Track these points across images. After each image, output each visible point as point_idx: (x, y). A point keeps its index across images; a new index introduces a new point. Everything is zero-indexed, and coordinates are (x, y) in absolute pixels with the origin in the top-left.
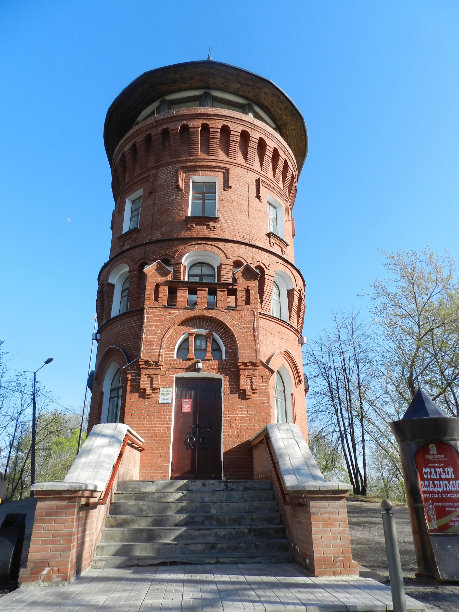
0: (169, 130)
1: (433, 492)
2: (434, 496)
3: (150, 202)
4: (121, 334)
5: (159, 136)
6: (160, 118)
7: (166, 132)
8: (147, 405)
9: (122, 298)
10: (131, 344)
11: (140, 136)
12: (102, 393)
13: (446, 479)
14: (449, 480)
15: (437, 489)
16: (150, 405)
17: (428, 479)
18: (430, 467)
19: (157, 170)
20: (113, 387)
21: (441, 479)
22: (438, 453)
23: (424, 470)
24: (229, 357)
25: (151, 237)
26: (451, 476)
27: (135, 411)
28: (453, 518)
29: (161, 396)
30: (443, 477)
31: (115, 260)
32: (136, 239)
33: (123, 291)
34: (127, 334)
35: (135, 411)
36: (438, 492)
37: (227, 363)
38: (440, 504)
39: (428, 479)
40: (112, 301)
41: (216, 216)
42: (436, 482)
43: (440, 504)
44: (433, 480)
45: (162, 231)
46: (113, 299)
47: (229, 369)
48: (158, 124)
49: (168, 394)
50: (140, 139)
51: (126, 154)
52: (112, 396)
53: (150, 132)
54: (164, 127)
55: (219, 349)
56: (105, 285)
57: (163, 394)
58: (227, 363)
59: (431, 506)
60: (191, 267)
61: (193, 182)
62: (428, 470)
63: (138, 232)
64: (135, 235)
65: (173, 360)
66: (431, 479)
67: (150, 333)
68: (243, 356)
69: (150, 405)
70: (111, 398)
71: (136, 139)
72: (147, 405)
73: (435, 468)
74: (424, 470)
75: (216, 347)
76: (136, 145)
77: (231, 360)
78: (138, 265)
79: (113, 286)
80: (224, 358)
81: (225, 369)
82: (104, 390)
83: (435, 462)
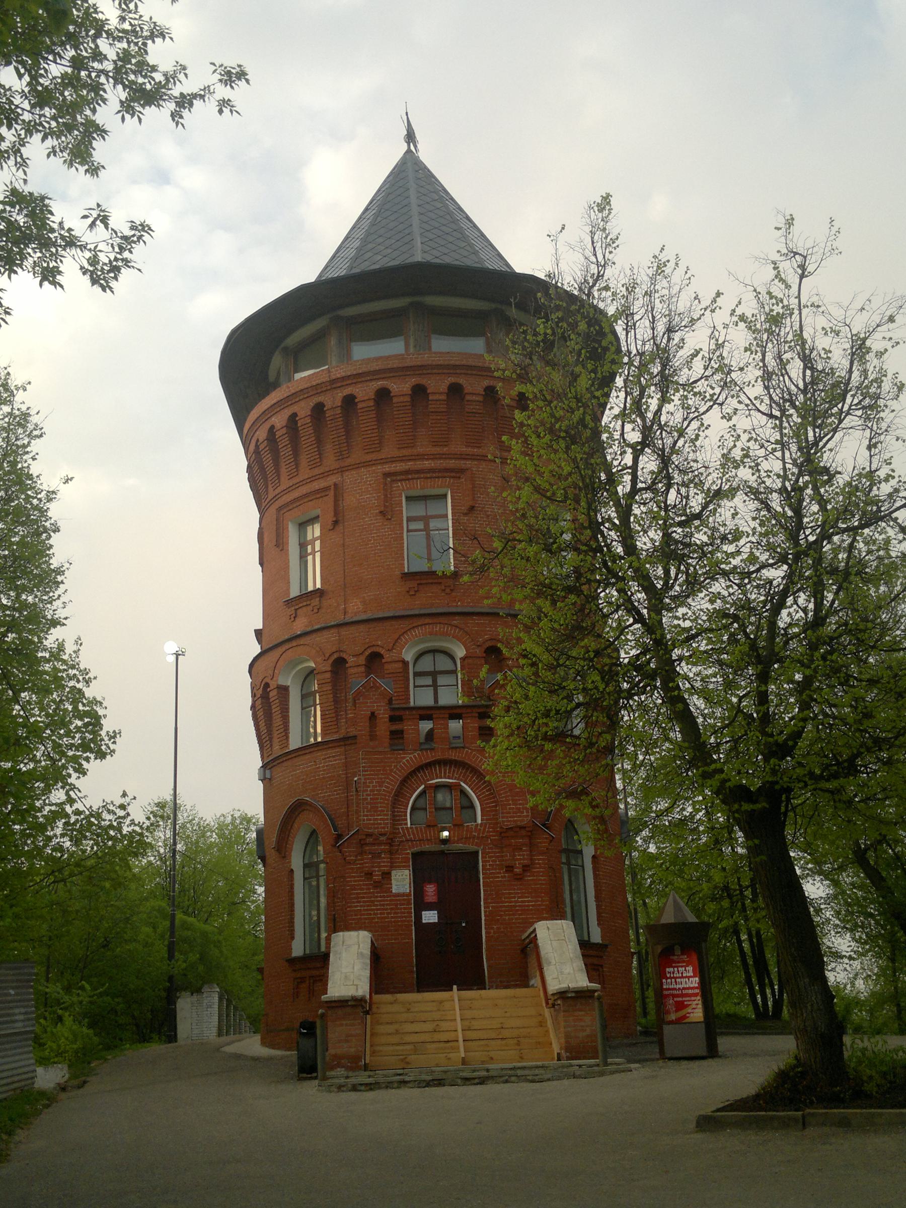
0: (356, 400)
1: (674, 989)
2: (675, 992)
4: (314, 776)
5: (339, 411)
6: (339, 376)
7: (349, 401)
8: (377, 897)
10: (333, 795)
11: (302, 404)
13: (686, 977)
14: (689, 977)
15: (678, 986)
16: (381, 897)
18: (674, 967)
20: (306, 861)
21: (682, 977)
22: (682, 954)
24: (487, 820)
27: (361, 906)
28: (690, 1011)
30: (684, 975)
31: (287, 646)
34: (324, 778)
35: (361, 906)
36: (679, 989)
37: (484, 830)
38: (680, 999)
40: (288, 716)
43: (680, 999)
46: (288, 712)
47: (487, 837)
48: (334, 386)
49: (404, 879)
51: (278, 434)
54: (347, 391)
55: (472, 807)
56: (272, 688)
58: (484, 830)
59: (671, 1001)
60: (416, 660)
61: (407, 498)
62: (671, 970)
64: (316, 602)
66: (674, 977)
67: (371, 791)
68: (507, 817)
69: (381, 897)
71: (295, 409)
72: (377, 897)
73: (678, 967)
75: (466, 804)
76: (296, 423)
77: (490, 824)
78: (330, 661)
80: (479, 821)
81: (483, 837)
83: (679, 962)
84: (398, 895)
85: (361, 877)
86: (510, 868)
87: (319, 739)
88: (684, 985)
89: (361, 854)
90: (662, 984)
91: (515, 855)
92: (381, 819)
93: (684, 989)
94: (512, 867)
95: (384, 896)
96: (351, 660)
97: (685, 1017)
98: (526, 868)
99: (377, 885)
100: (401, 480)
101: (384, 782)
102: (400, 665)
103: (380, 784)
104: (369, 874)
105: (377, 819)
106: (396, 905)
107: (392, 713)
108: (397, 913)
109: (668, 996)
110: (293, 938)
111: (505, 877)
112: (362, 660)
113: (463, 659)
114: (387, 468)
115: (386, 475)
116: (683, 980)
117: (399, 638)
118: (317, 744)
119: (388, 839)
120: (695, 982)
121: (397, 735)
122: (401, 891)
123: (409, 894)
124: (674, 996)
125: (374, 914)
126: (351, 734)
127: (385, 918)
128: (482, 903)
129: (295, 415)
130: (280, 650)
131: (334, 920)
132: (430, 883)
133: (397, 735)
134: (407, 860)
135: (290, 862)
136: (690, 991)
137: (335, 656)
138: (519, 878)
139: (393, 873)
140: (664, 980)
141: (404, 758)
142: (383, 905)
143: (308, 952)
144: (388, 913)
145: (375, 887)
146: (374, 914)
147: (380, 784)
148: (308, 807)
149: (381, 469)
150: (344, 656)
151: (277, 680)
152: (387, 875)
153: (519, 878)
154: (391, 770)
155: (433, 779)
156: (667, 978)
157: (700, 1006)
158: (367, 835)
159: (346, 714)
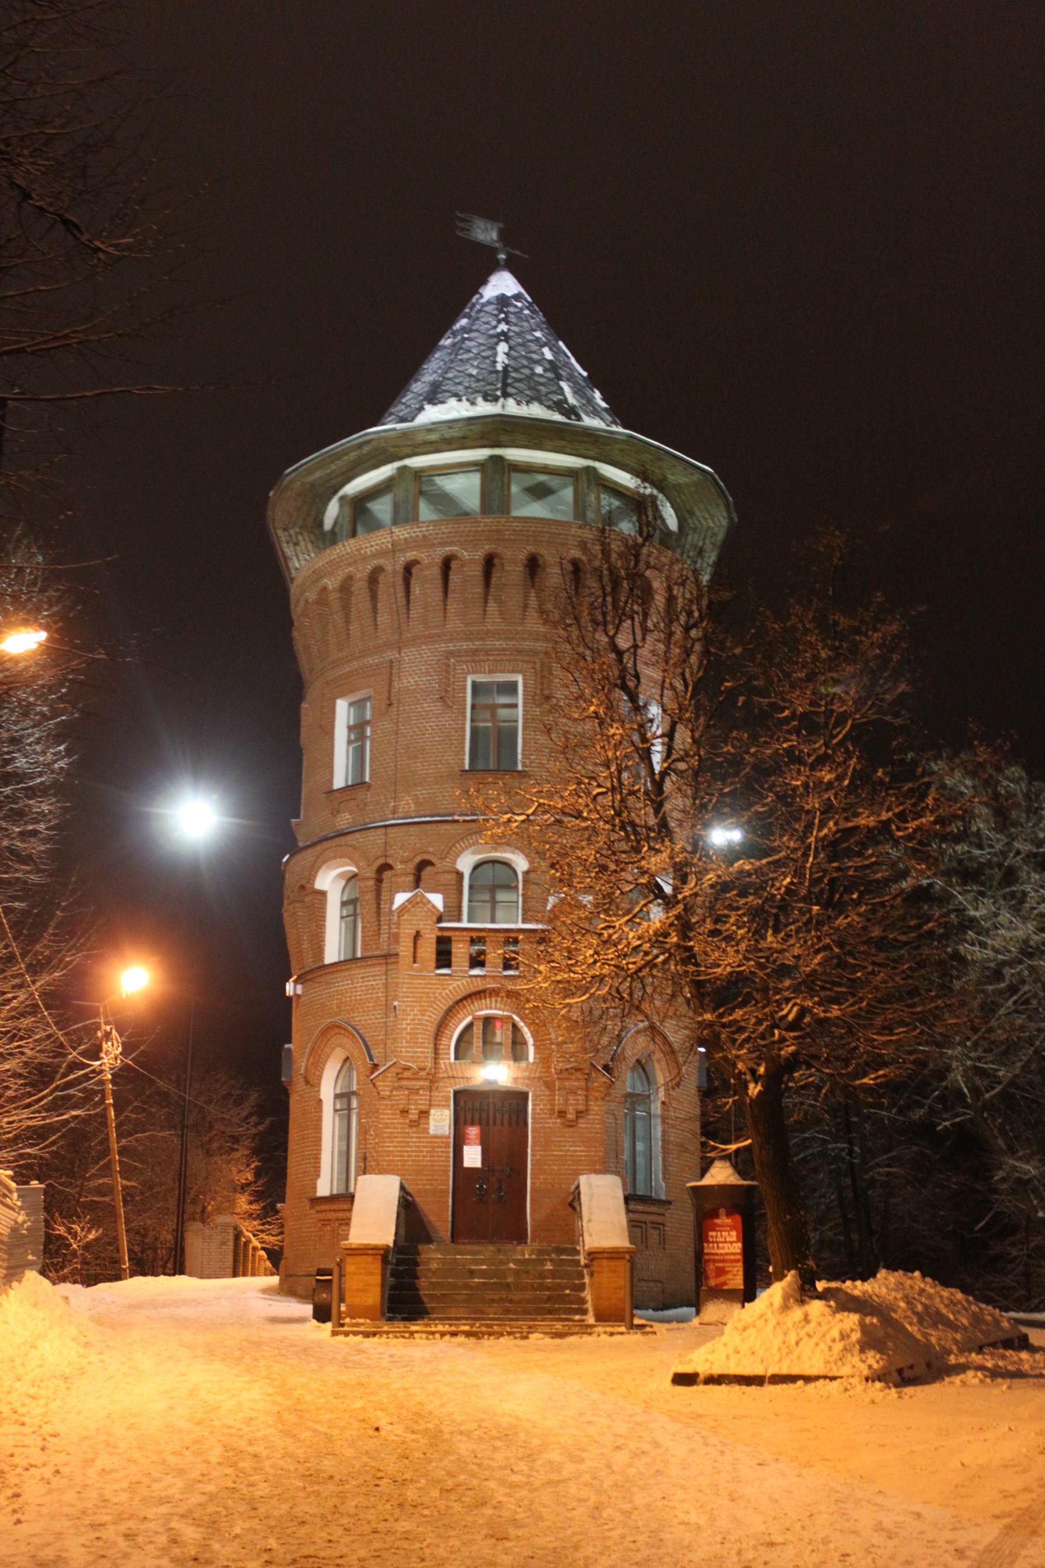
1: (717, 1254)
2: (717, 1257)
3: (387, 725)
9: (342, 917)
12: (320, 1101)
14: (731, 1243)
17: (713, 1242)
19: (400, 653)
20: (338, 1091)
21: (725, 1242)
23: (711, 1233)
25: (395, 806)
26: (734, 1239)
29: (432, 1122)
32: (366, 805)
33: (344, 904)
38: (721, 1265)
39: (713, 1242)
41: (520, 768)
42: (721, 1245)
43: (721, 1265)
44: (717, 1243)
45: (416, 795)
49: (443, 1120)
50: (361, 573)
52: (338, 1107)
53: (381, 561)
57: (436, 1120)
63: (368, 790)
65: (450, 1064)
67: (412, 1020)
70: (336, 1111)
74: (711, 1233)
78: (375, 867)
79: (323, 894)
82: (323, 1097)
84: (436, 1137)
85: (395, 1114)
86: (562, 1114)
87: (359, 955)
88: (726, 1251)
89: (398, 1088)
90: (703, 1247)
91: (567, 1100)
92: (422, 1052)
93: (727, 1254)
94: (565, 1112)
95: (420, 1138)
96: (399, 867)
97: (725, 1283)
98: (579, 1114)
99: (414, 1124)
100: (466, 662)
101: (426, 1011)
102: (454, 876)
103: (423, 1012)
104: (405, 1112)
105: (416, 1052)
106: (434, 1147)
107: (440, 934)
108: (434, 1156)
109: (709, 1261)
110: (318, 1176)
111: (555, 1123)
112: (411, 867)
113: (526, 873)
114: (451, 646)
115: (449, 654)
116: (726, 1245)
117: (454, 845)
118: (355, 959)
119: (428, 1074)
120: (738, 1247)
121: (444, 958)
122: (440, 1132)
123: (448, 1137)
124: (715, 1261)
125: (409, 1156)
126: (392, 952)
127: (419, 1161)
128: (529, 1151)
129: (350, 578)
130: (319, 848)
131: (365, 1159)
132: (473, 1124)
133: (444, 958)
134: (447, 1099)
135: (319, 1091)
136: (732, 1257)
137: (381, 861)
138: (571, 1125)
139: (432, 1112)
140: (706, 1245)
141: (450, 985)
142: (419, 1147)
143: (335, 1192)
144: (424, 1156)
145: (411, 1126)
146: (409, 1156)
147: (423, 1012)
148: (343, 1032)
149: (442, 647)
150: (390, 861)
151: (313, 884)
152: (424, 1114)
153: (571, 1125)
154: (435, 998)
155: (482, 1010)
156: (708, 1242)
157: (741, 1273)
158: (404, 1069)
159: (390, 928)
